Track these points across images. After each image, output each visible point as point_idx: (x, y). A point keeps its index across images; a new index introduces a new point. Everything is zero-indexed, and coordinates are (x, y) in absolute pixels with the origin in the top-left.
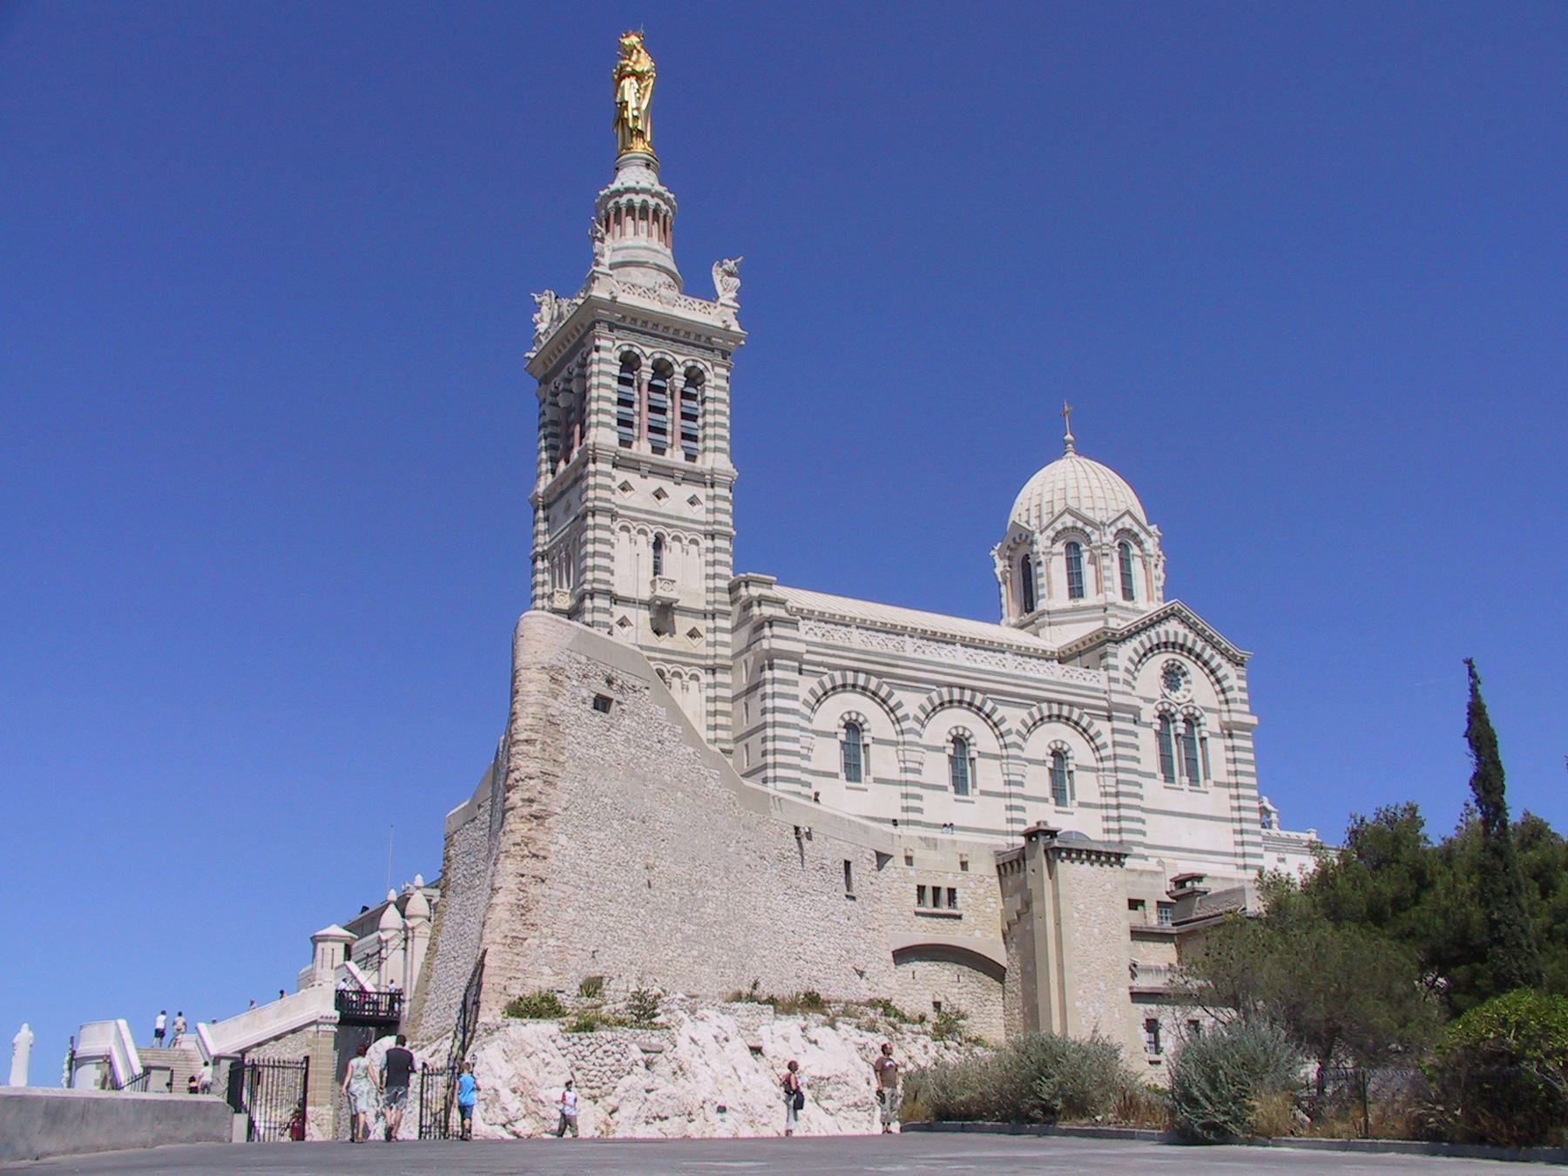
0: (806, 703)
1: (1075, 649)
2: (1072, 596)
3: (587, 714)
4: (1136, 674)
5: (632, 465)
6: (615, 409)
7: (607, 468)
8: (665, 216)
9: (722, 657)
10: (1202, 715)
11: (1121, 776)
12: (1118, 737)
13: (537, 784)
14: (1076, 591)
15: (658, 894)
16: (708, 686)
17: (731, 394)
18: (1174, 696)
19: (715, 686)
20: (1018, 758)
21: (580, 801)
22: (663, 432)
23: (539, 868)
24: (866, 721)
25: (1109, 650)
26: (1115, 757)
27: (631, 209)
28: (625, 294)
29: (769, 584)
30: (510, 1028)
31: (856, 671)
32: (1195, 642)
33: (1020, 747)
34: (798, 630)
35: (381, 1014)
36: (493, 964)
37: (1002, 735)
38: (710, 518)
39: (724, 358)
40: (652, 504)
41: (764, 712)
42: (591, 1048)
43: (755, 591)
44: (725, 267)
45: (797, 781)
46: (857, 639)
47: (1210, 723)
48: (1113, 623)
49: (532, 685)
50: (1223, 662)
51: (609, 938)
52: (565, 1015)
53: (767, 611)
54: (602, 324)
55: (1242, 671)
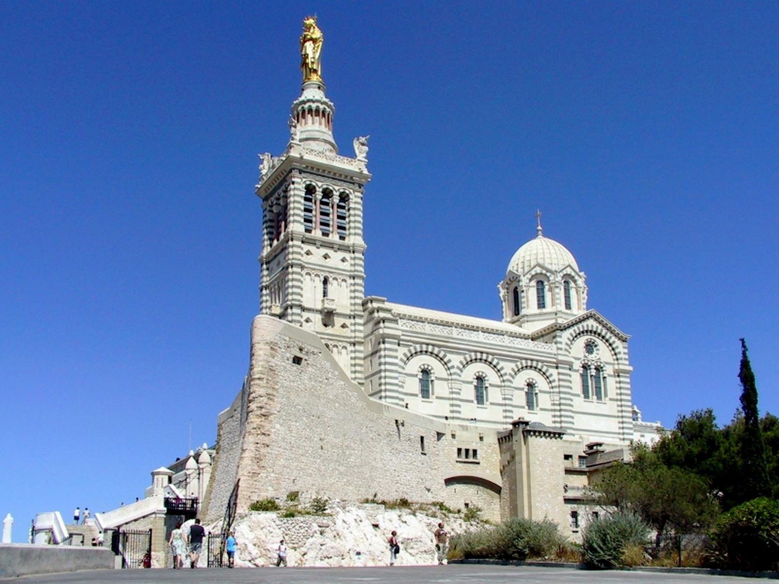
0: (401, 360)
1: (540, 334)
3: (290, 365)
4: (571, 346)
5: (312, 242)
6: (302, 214)
7: (299, 243)
8: (328, 115)
9: (358, 337)
10: (604, 366)
11: (562, 395)
12: (561, 377)
13: (265, 399)
14: (541, 304)
15: (326, 452)
16: (352, 352)
17: (363, 206)
18: (590, 357)
19: (355, 352)
20: (510, 387)
21: (286, 408)
22: (328, 225)
23: (266, 440)
24: (432, 369)
25: (558, 334)
26: (559, 386)
27: (310, 111)
28: (307, 155)
29: (383, 301)
30: (252, 516)
31: (427, 344)
32: (602, 330)
33: (511, 381)
34: (398, 324)
35: (188, 509)
36: (244, 485)
37: (502, 376)
38: (353, 268)
39: (360, 187)
40: (323, 262)
41: (380, 364)
42: (293, 525)
43: (375, 305)
44: (360, 141)
45: (397, 398)
46: (428, 328)
47: (608, 370)
48: (560, 321)
49: (261, 351)
50: (616, 340)
51: (301, 473)
52: (279, 509)
53: (382, 315)
54: (296, 170)
55: (626, 344)
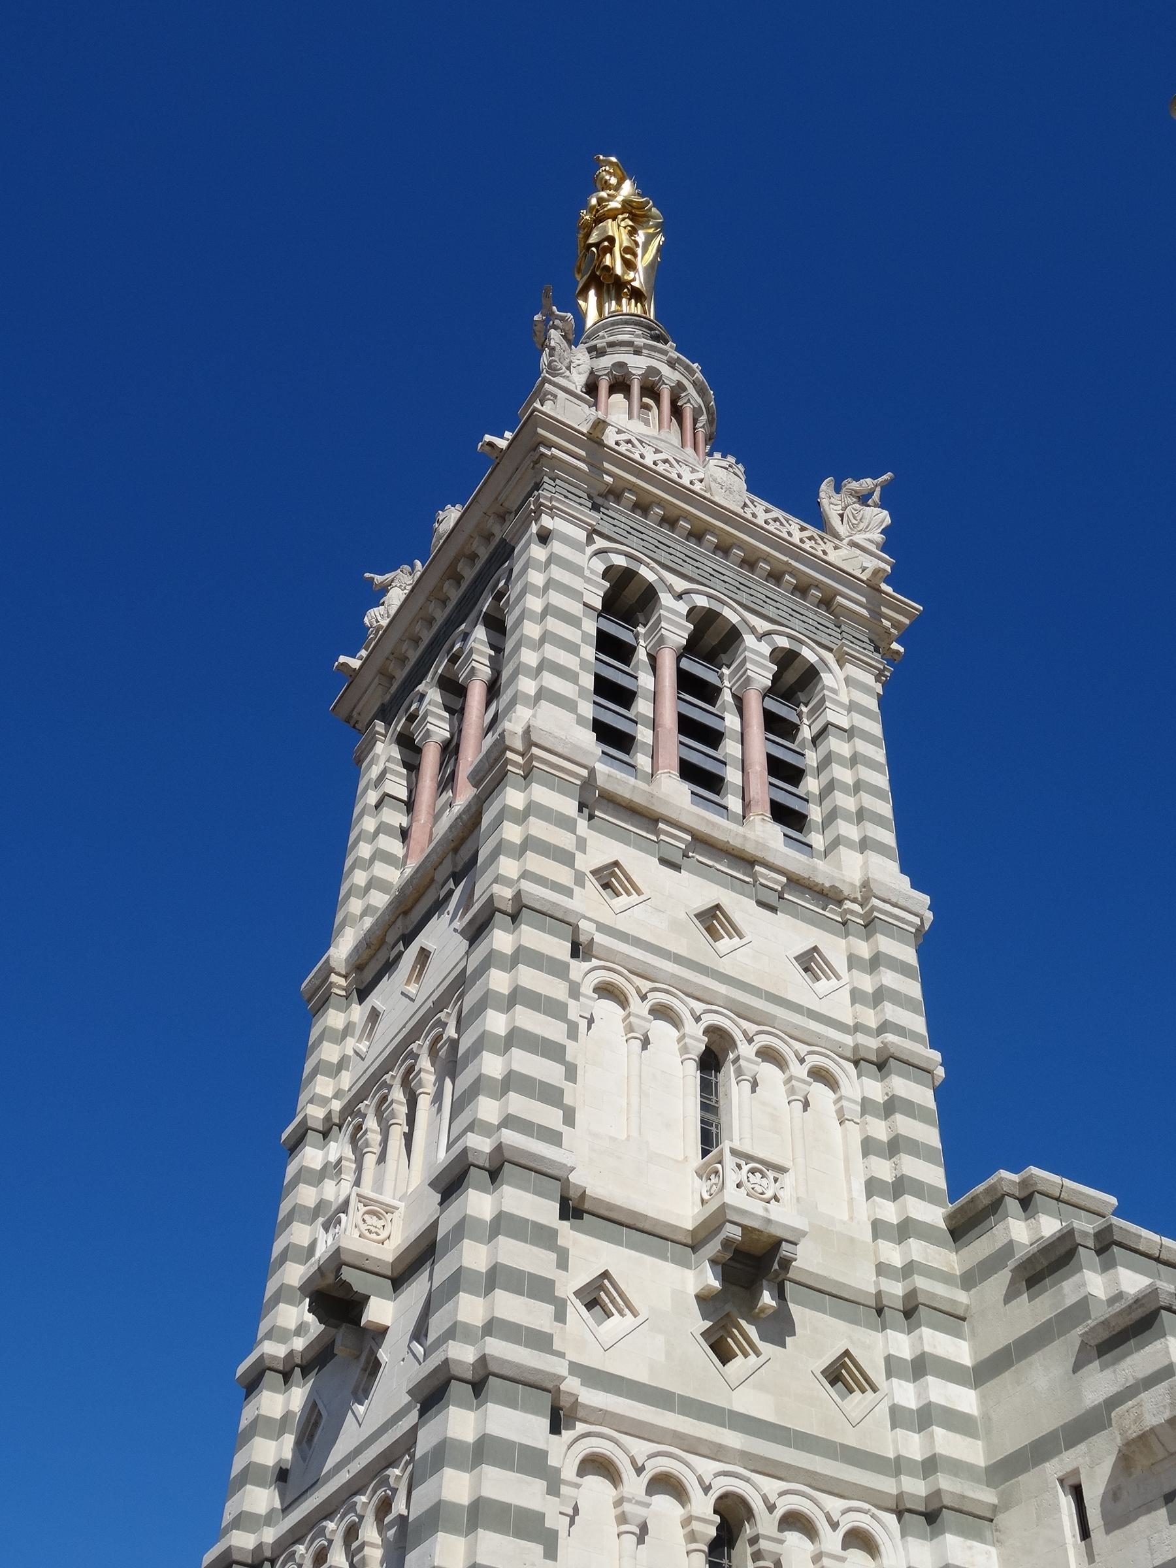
9: (957, 1467)
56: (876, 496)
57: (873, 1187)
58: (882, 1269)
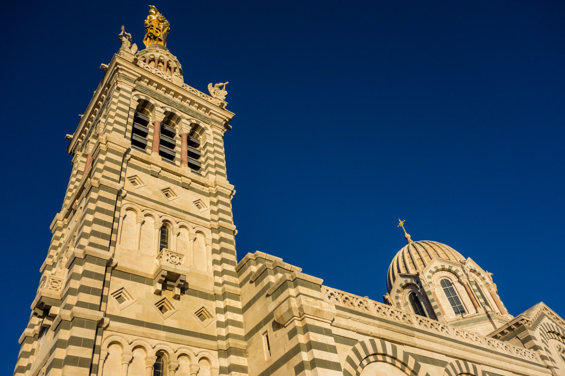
2: (457, 313)
56: (224, 88)
57: (215, 262)
58: (216, 284)
